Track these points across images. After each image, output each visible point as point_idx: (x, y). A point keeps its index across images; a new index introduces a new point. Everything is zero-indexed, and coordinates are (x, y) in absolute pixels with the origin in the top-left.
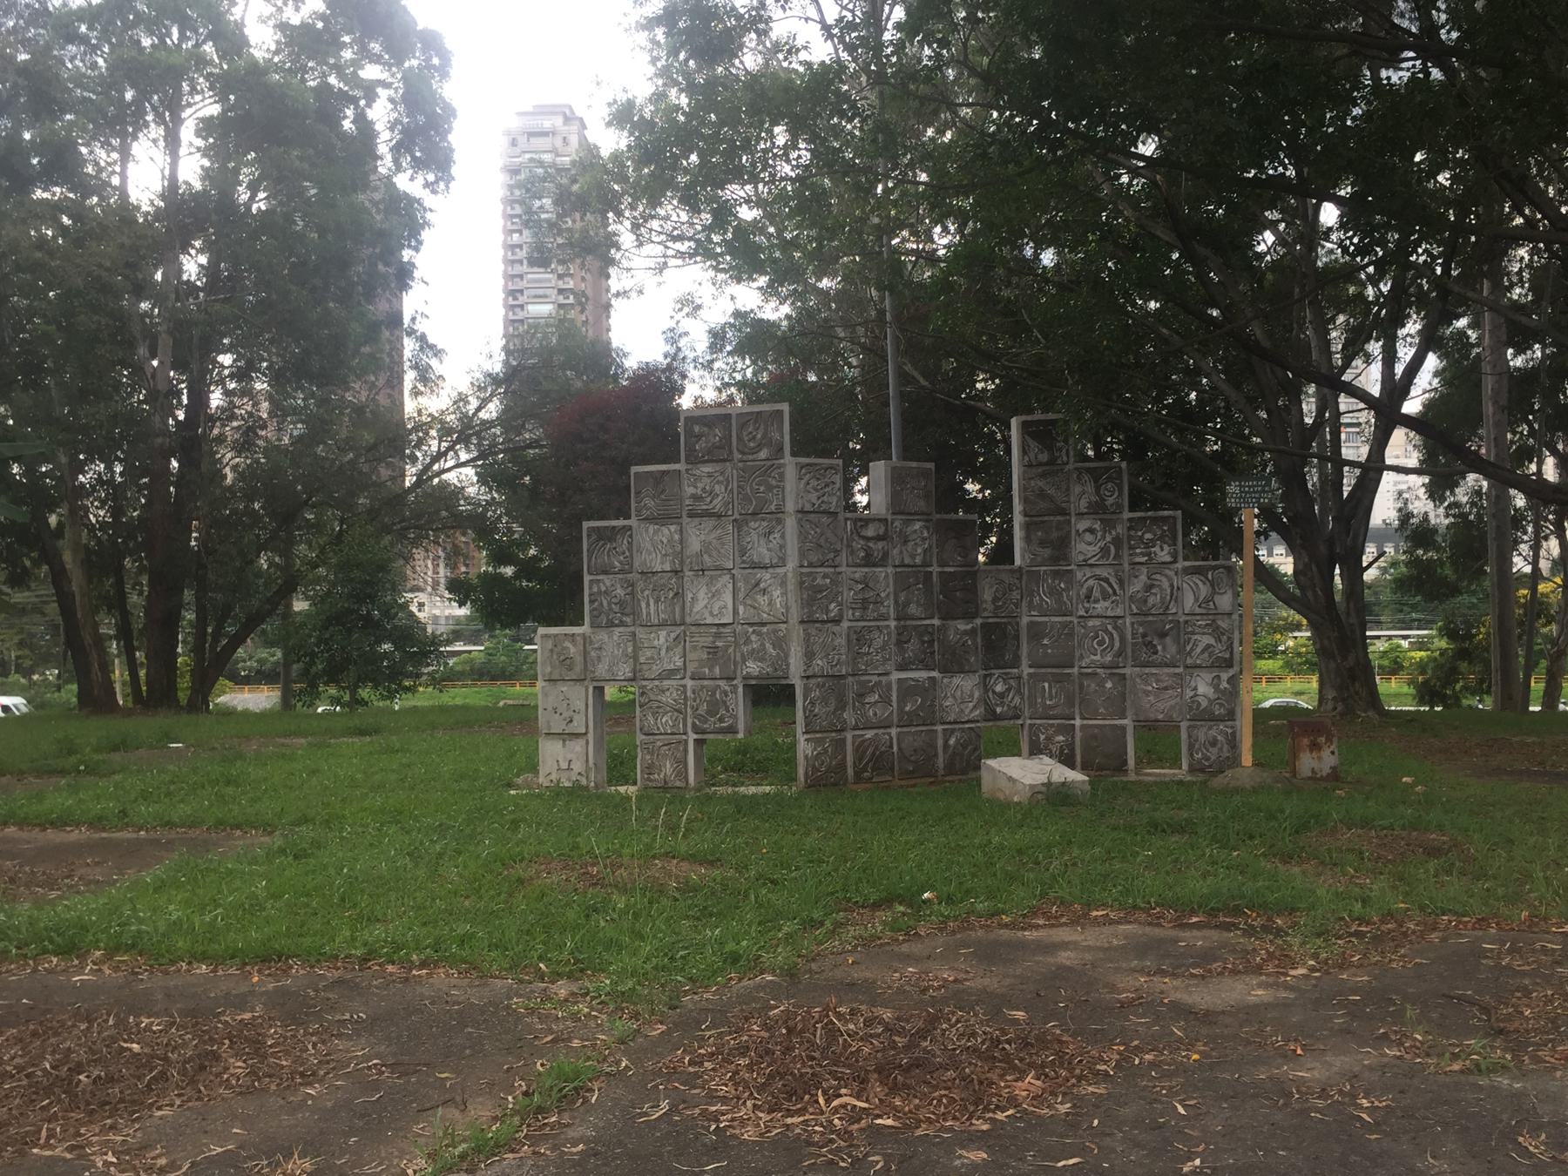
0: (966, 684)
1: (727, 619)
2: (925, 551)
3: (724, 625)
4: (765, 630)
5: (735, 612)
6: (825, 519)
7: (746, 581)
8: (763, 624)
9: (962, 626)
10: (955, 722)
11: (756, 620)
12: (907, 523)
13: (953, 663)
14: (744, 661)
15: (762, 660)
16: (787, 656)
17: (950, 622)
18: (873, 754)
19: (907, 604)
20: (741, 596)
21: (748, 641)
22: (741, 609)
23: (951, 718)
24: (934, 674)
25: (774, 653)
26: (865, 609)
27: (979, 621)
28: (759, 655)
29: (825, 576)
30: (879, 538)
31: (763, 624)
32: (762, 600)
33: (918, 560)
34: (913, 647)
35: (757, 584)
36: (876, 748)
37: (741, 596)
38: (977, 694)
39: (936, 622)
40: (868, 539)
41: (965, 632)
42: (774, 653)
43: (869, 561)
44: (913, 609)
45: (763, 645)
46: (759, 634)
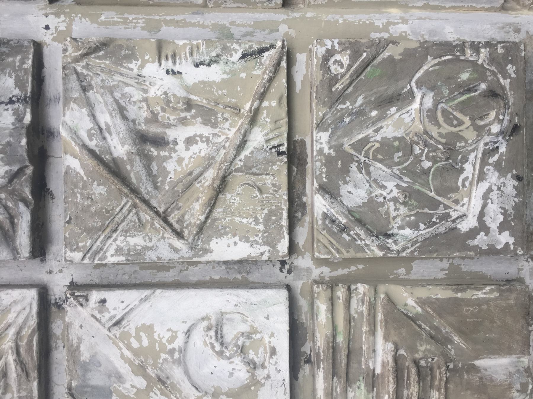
1: (267, 314)
3: (297, 332)
4: (320, 143)
5: (239, 276)
7: (109, 225)
8: (294, 156)
11: (277, 176)
14: (452, 241)
15: (451, 157)
16: (446, 47)
20: (165, 247)
21: (370, 220)
22: (226, 249)
25: (422, 100)
28: (432, 174)
31: (294, 156)
32: (190, 149)
35: (114, 170)
37: (165, 247)
42: (422, 100)
45: (386, 151)
46: (339, 165)
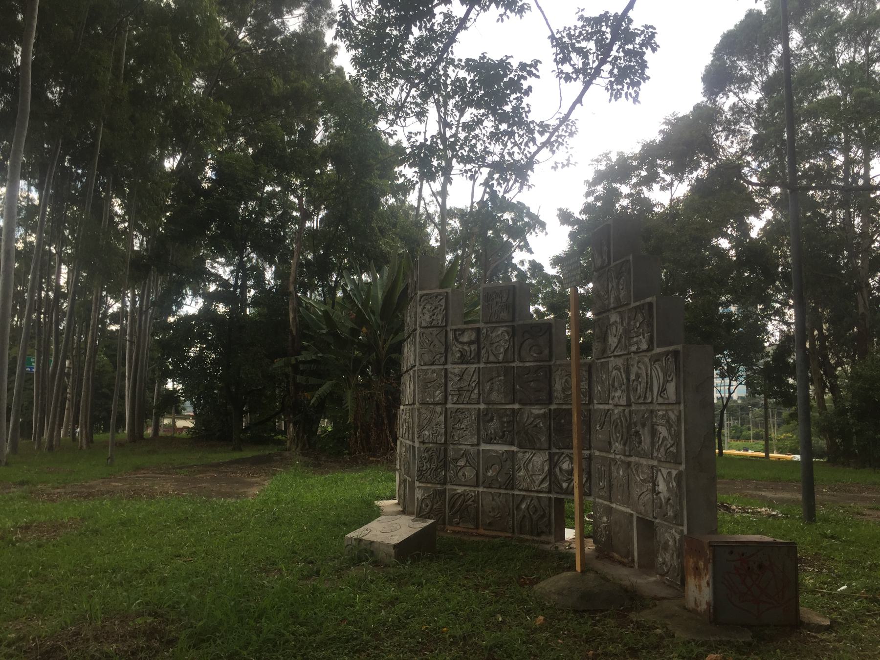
0: (539, 459)
2: (506, 351)
6: (435, 331)
9: (537, 410)
10: (527, 490)
12: (494, 329)
13: (529, 442)
17: (527, 408)
18: (461, 505)
19: (491, 390)
23: (524, 485)
24: (514, 449)
26: (460, 395)
27: (553, 407)
29: (434, 371)
30: (470, 343)
33: (501, 358)
34: (494, 425)
36: (464, 501)
38: (546, 468)
39: (516, 406)
40: (461, 343)
41: (538, 416)
43: (463, 360)
44: (494, 396)
